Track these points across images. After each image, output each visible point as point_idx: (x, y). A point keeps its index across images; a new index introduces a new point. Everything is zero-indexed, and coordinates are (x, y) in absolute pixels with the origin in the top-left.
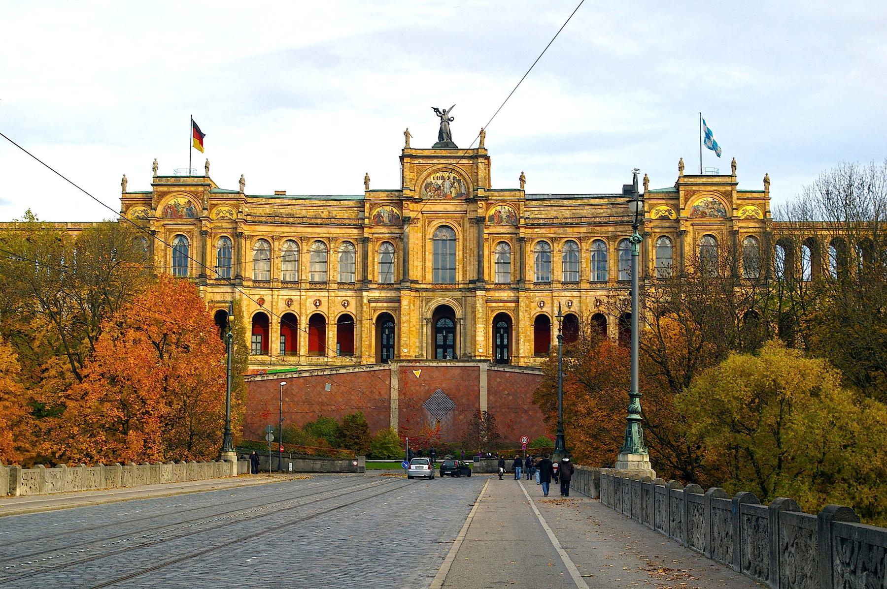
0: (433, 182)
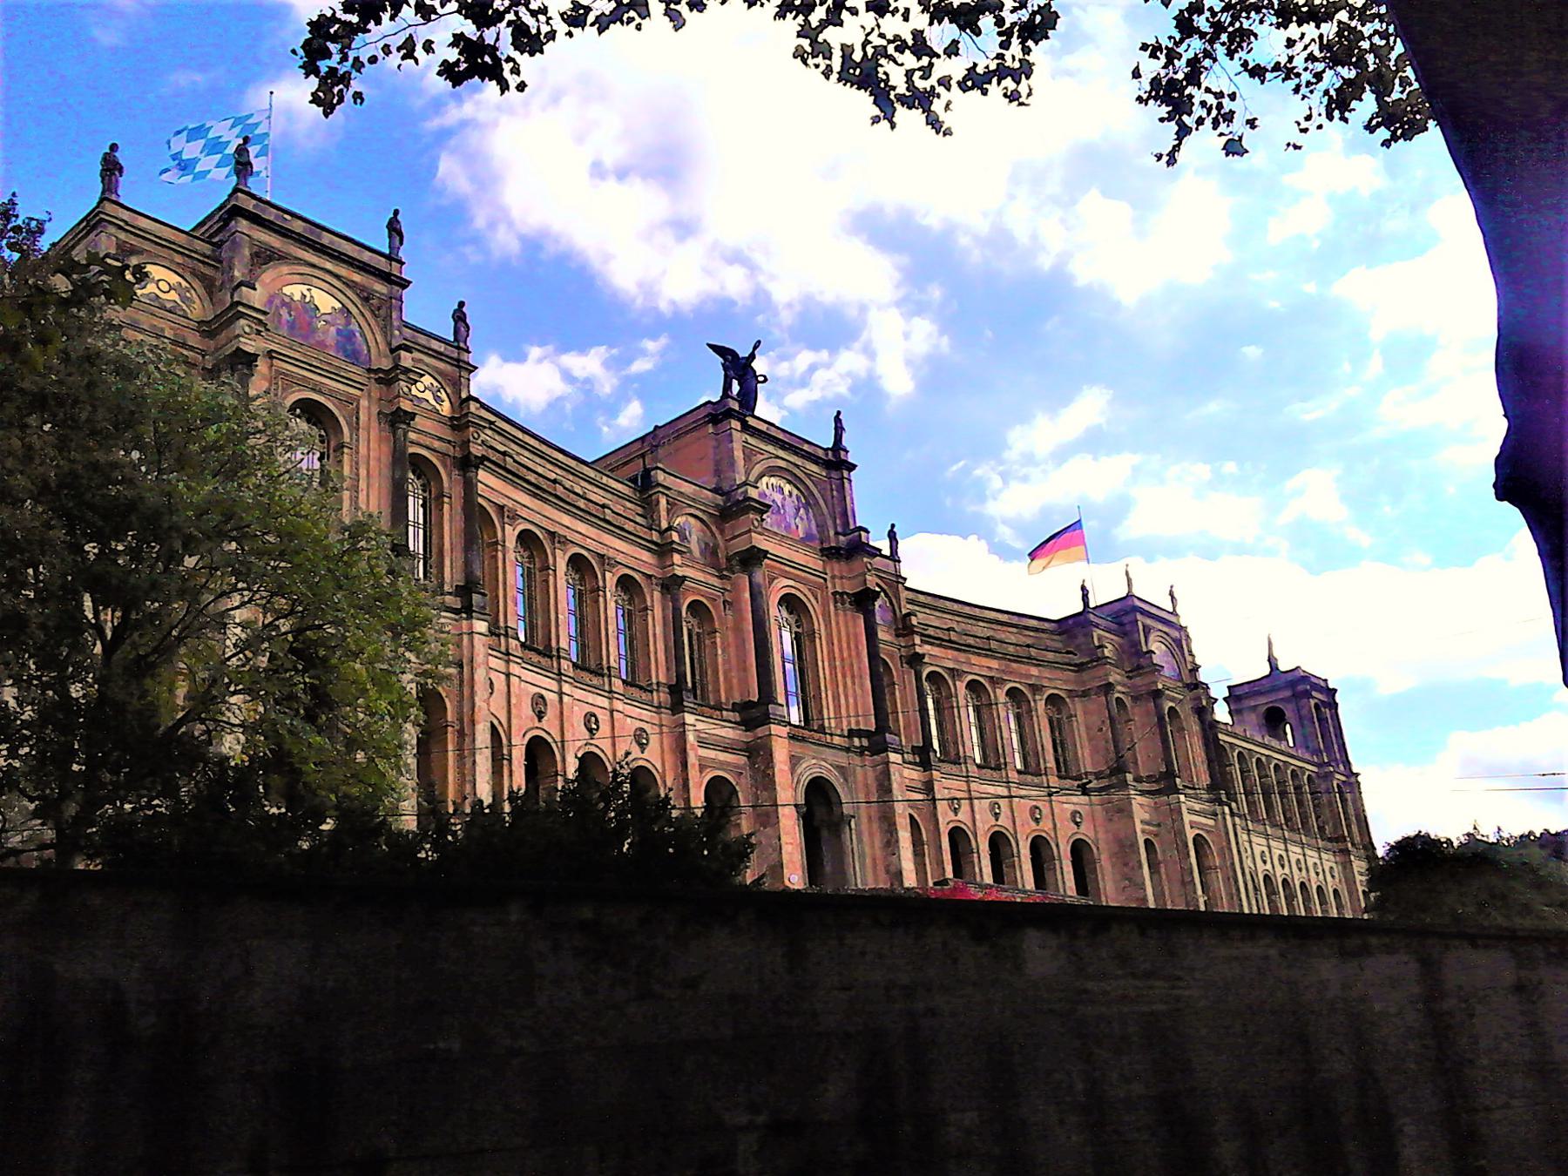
0: (767, 492)
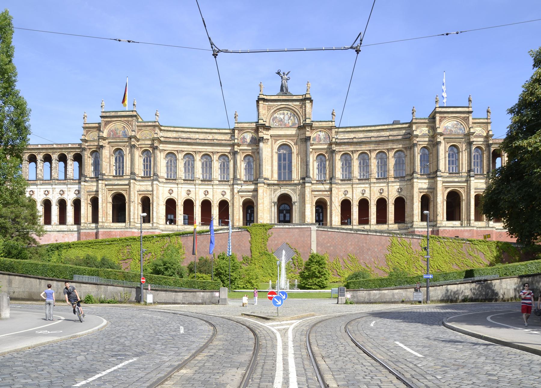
0: (278, 116)
